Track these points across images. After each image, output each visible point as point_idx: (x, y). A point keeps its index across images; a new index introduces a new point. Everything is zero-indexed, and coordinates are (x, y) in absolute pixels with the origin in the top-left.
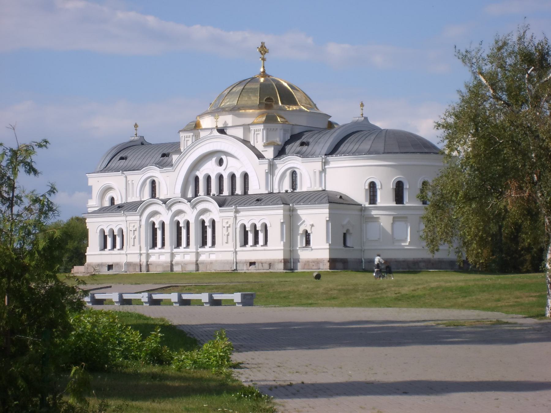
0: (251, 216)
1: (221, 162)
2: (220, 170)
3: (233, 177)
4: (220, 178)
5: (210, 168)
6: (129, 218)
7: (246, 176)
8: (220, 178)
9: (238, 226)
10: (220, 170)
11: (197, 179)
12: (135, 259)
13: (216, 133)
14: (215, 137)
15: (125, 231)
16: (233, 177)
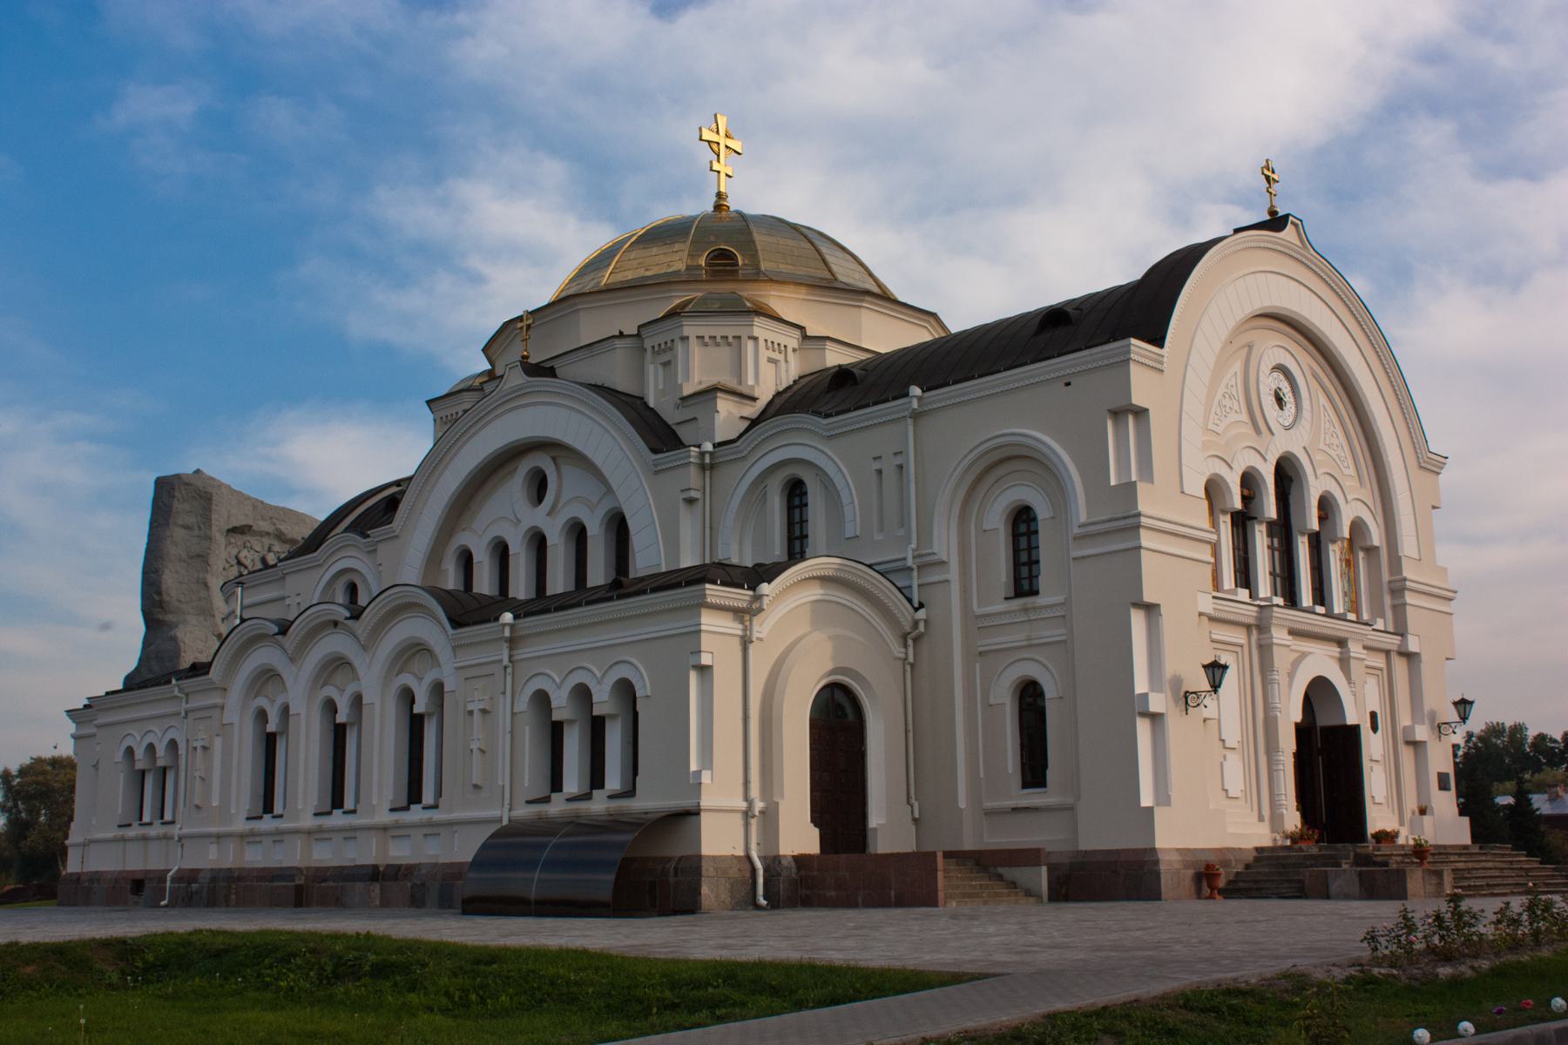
0: (579, 658)
1: (539, 486)
2: (537, 517)
3: (578, 534)
4: (539, 542)
5: (508, 514)
6: (196, 702)
7: (619, 527)
8: (539, 542)
9: (523, 703)
10: (537, 517)
11: (466, 560)
12: (211, 858)
13: (517, 378)
14: (519, 393)
15: (182, 751)
16: (578, 534)
